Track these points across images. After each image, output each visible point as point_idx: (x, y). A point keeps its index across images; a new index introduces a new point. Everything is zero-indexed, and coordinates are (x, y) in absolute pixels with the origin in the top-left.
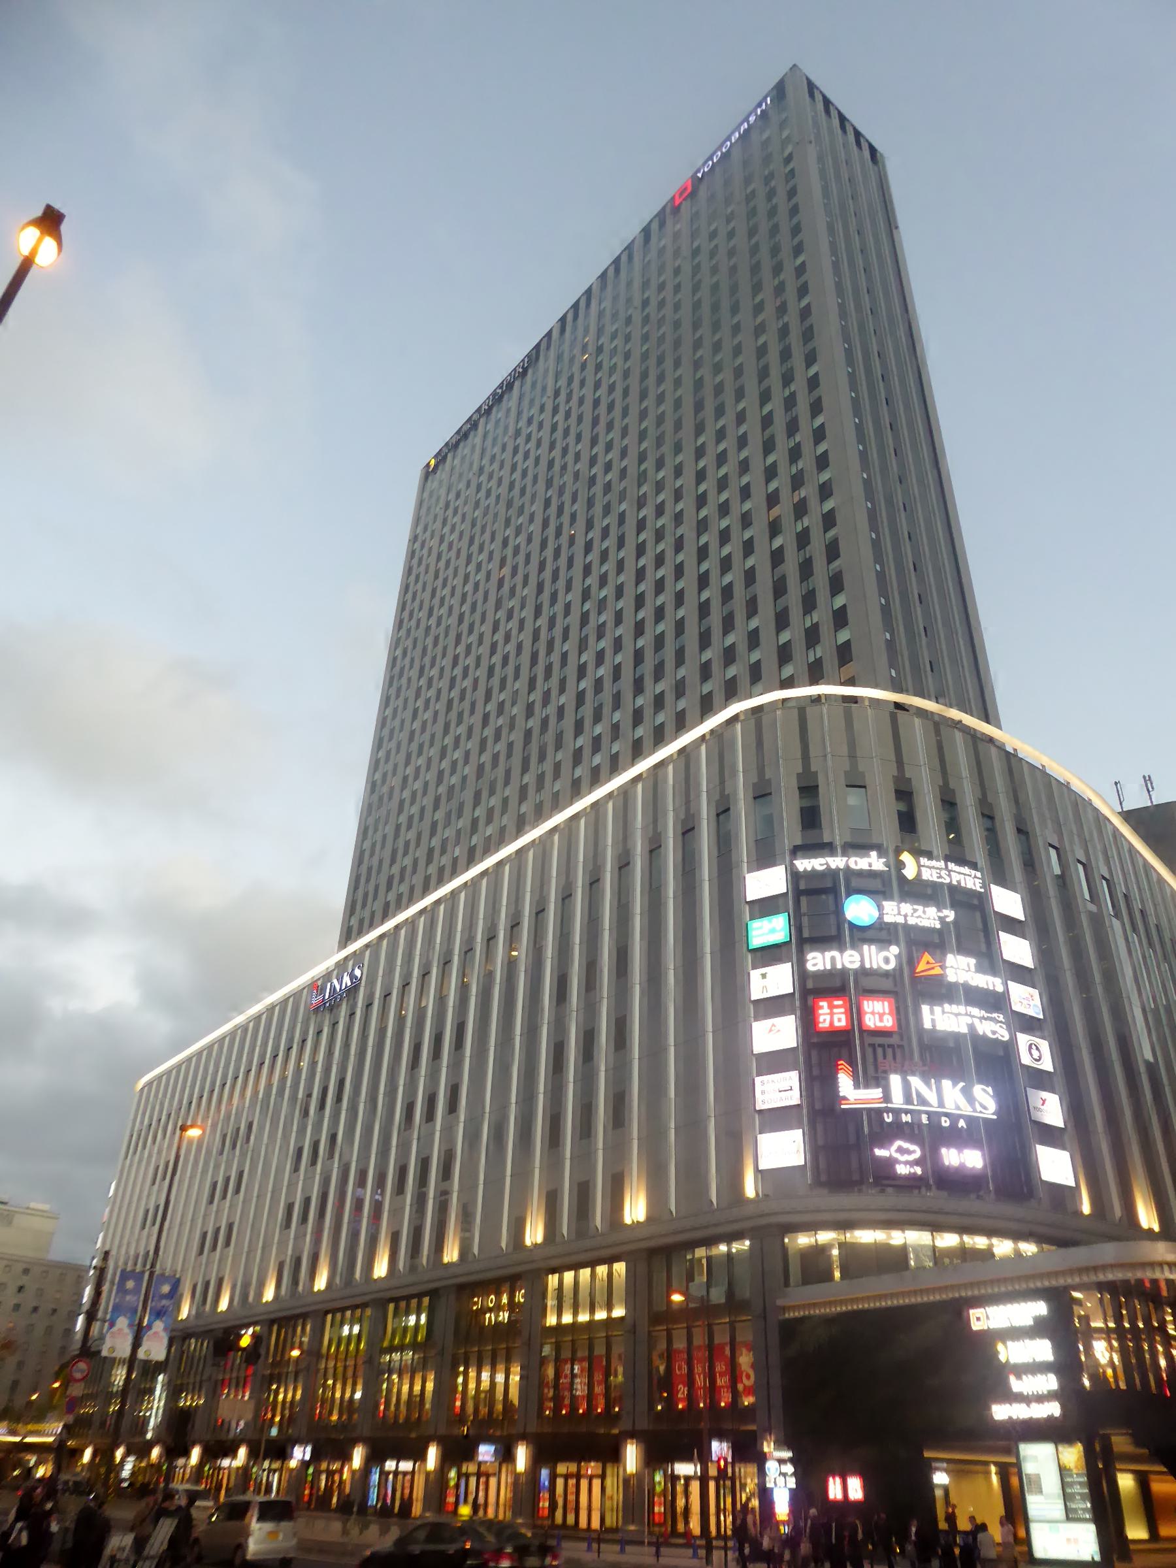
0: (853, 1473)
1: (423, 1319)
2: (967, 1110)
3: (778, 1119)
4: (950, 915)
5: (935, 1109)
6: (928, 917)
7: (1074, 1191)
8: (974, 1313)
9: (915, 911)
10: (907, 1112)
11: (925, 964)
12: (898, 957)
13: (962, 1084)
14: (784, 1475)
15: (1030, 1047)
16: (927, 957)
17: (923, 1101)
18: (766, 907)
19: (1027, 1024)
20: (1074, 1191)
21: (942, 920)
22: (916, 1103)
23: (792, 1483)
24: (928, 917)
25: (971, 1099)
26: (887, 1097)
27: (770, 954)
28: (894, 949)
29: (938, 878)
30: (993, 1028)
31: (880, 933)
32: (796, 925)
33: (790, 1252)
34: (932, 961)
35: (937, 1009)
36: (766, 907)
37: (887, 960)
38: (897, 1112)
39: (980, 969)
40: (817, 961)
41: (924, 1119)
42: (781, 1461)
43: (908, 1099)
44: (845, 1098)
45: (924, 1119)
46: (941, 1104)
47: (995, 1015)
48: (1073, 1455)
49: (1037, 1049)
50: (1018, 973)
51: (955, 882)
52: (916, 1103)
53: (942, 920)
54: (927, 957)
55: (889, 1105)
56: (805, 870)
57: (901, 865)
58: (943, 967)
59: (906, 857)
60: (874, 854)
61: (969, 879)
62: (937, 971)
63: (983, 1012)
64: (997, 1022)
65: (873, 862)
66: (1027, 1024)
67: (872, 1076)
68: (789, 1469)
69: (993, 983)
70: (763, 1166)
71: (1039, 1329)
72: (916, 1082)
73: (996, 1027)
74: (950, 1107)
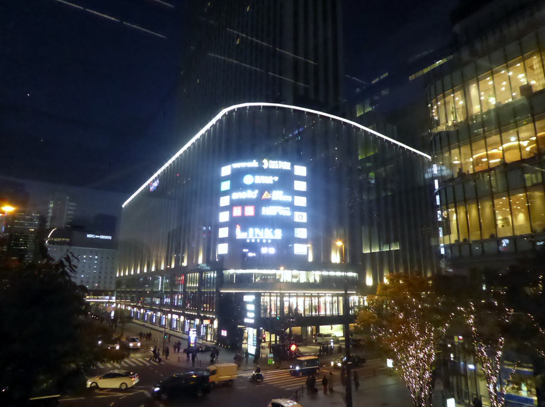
0: (226, 330)
1: (183, 277)
2: (273, 238)
3: (223, 240)
4: (276, 179)
5: (262, 237)
6: (269, 180)
7: (306, 257)
8: (245, 297)
9: (265, 178)
10: (253, 239)
11: (266, 195)
12: (258, 194)
13: (272, 230)
14: (194, 334)
15: (299, 216)
16: (266, 192)
17: (258, 236)
18: (226, 178)
19: (300, 209)
20: (306, 257)
21: (274, 181)
22: (256, 235)
23: (195, 335)
24: (269, 180)
25: (273, 233)
26: (248, 236)
27: (226, 193)
28: (257, 191)
29: (275, 166)
30: (285, 212)
31: (253, 187)
32: (232, 185)
33: (225, 275)
34: (268, 193)
35: (267, 208)
36: (226, 178)
37: (254, 195)
38: (251, 240)
39: (284, 194)
40: (237, 196)
41: (258, 241)
42: (194, 331)
43: (254, 236)
44: (237, 236)
45: (258, 241)
46: (264, 236)
47: (287, 208)
48: (255, 331)
49: (302, 216)
50: (300, 194)
51: (280, 168)
52: (256, 235)
53: (274, 181)
54: (266, 192)
55: (248, 237)
56: (235, 168)
57: (263, 164)
58: (271, 195)
59: (265, 161)
60: (255, 161)
61: (285, 165)
62: (269, 197)
63: (283, 208)
64: (286, 210)
65: (254, 164)
66: (300, 209)
67: (244, 229)
68: (195, 332)
69: (288, 198)
70: (219, 253)
71: (253, 302)
72: (257, 230)
73: (286, 211)
74: (266, 237)
